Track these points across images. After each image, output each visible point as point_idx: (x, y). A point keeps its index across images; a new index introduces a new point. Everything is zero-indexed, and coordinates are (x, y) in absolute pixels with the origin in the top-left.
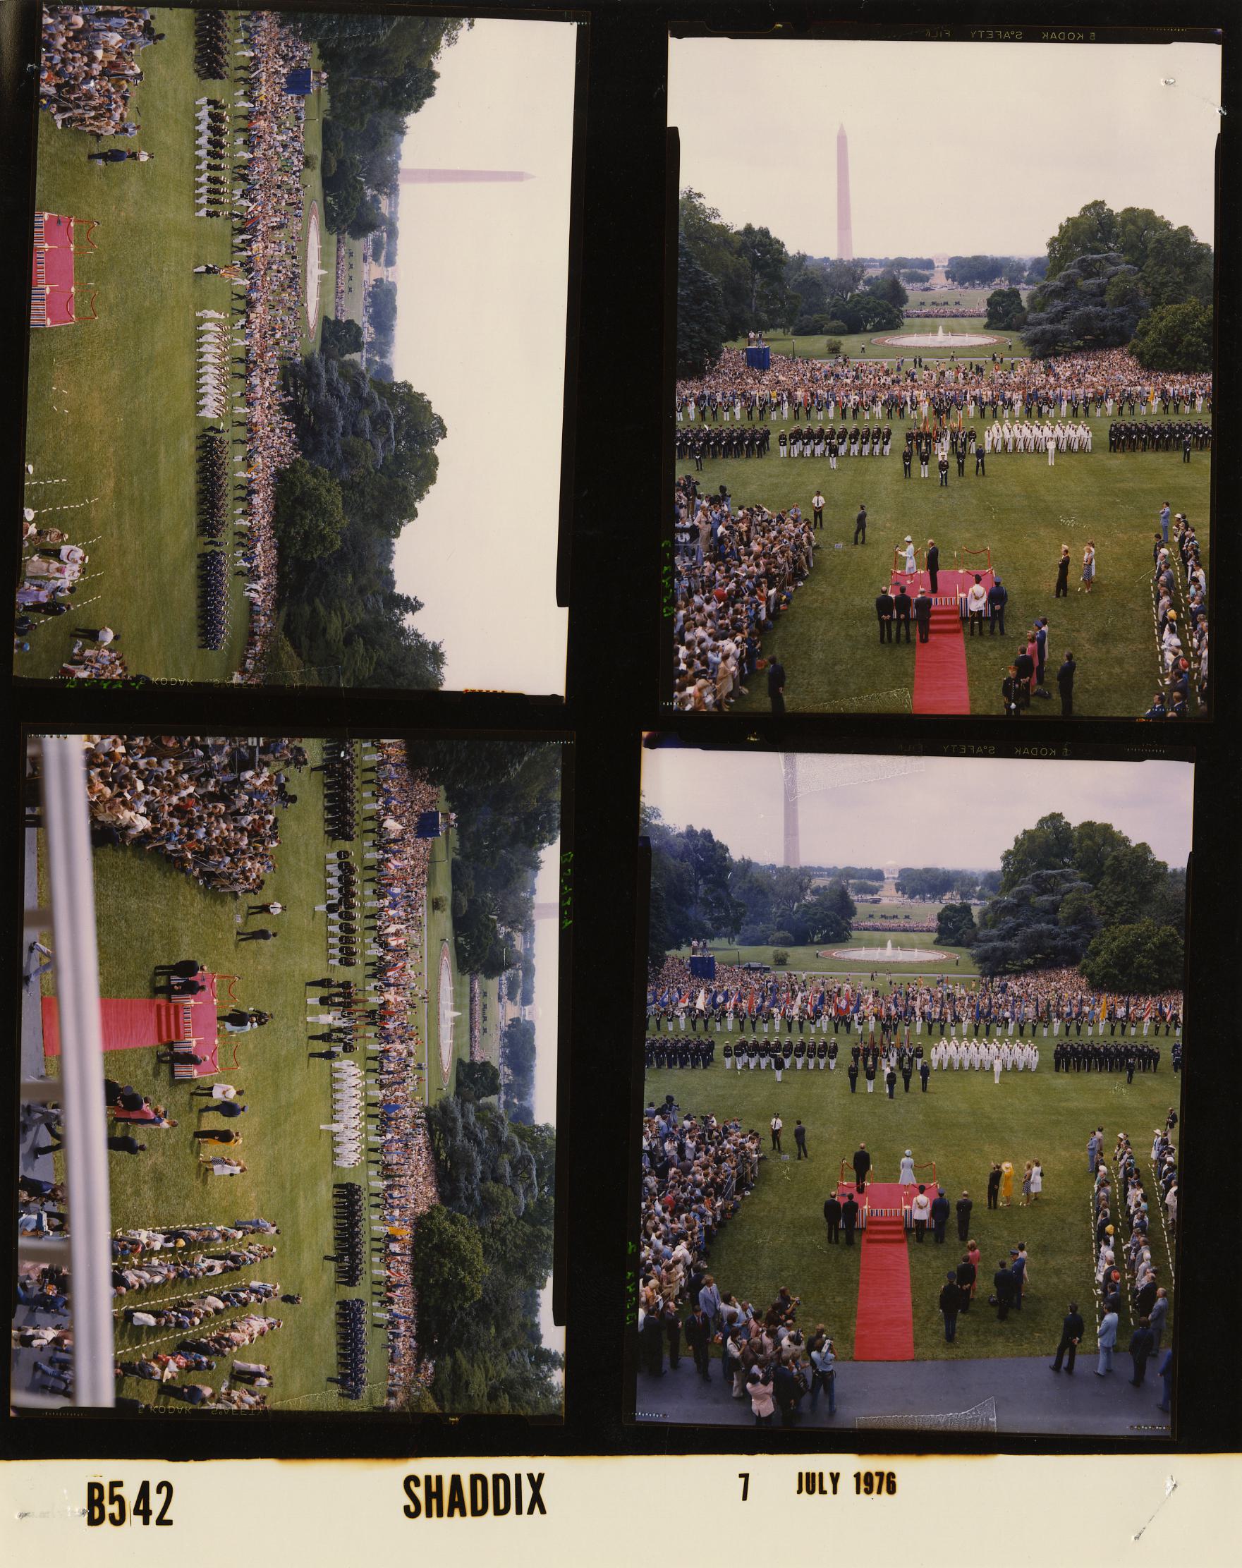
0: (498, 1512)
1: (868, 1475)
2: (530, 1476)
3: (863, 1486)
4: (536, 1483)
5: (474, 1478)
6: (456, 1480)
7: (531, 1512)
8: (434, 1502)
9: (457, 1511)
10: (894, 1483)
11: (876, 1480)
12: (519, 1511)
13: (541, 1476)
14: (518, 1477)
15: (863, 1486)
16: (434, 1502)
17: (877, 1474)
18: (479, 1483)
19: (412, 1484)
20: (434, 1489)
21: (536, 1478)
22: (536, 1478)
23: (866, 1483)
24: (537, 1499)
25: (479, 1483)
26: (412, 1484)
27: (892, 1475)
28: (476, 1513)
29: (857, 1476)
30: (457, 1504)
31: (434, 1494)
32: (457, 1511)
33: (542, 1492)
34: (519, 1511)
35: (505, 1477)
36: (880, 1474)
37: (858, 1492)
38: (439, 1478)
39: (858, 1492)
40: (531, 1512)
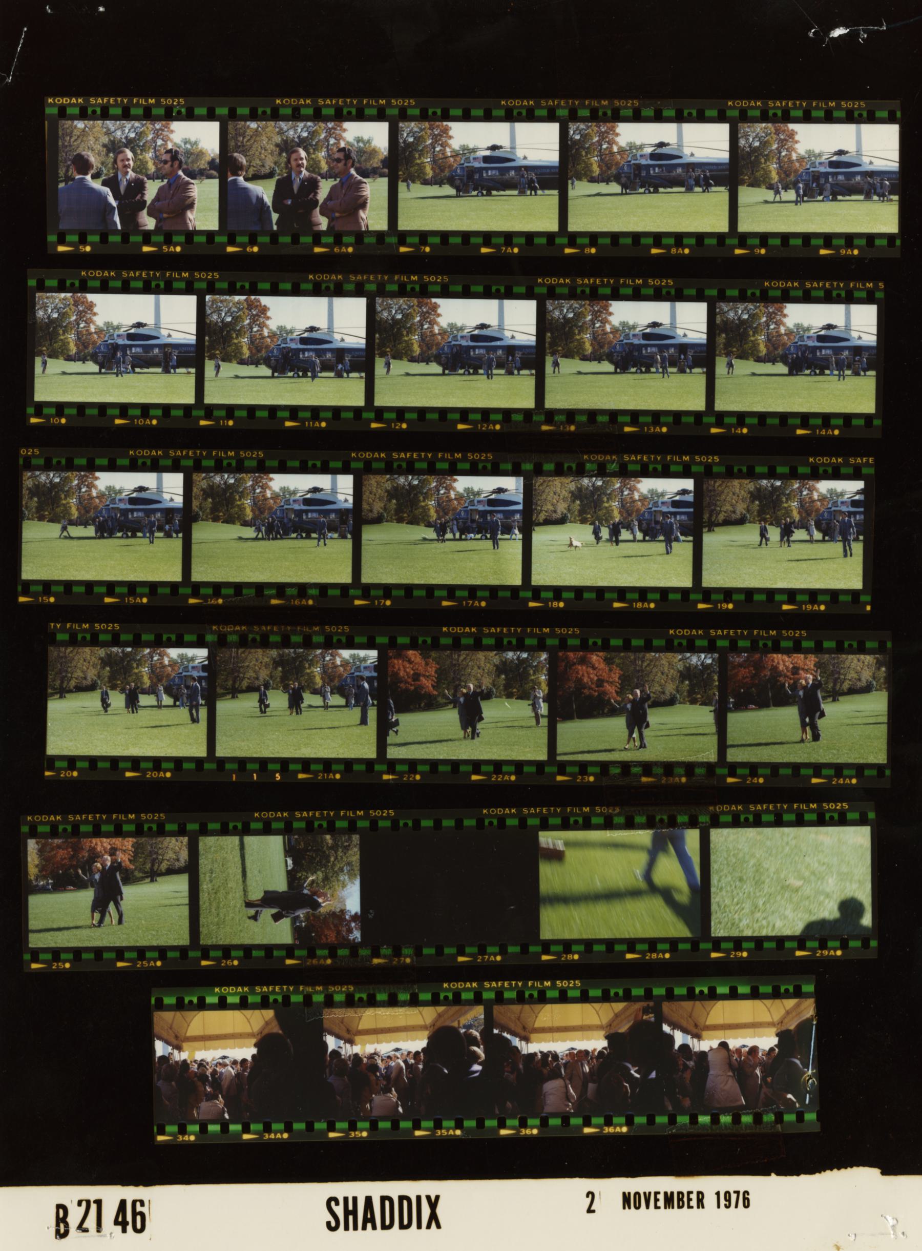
0: (402, 1227)
1: (727, 1193)
2: (428, 1197)
3: (723, 1202)
4: (433, 1204)
5: (383, 1199)
6: (369, 1200)
7: (429, 1227)
8: (351, 1218)
9: (369, 1225)
10: (748, 1199)
11: (734, 1197)
12: (419, 1226)
13: (437, 1197)
14: (419, 1198)
15: (723, 1202)
16: (351, 1218)
17: (735, 1192)
18: (387, 1203)
19: (333, 1203)
20: (351, 1207)
21: (433, 1199)
22: (433, 1199)
23: (726, 1199)
24: (434, 1217)
25: (387, 1203)
26: (333, 1203)
27: (746, 1192)
28: (384, 1227)
29: (718, 1194)
30: (369, 1220)
31: (350, 1212)
32: (369, 1225)
33: (439, 1211)
34: (419, 1226)
35: (391, 1200)
36: (737, 1192)
37: (719, 1207)
38: (355, 1199)
39: (719, 1207)
40: (429, 1227)
